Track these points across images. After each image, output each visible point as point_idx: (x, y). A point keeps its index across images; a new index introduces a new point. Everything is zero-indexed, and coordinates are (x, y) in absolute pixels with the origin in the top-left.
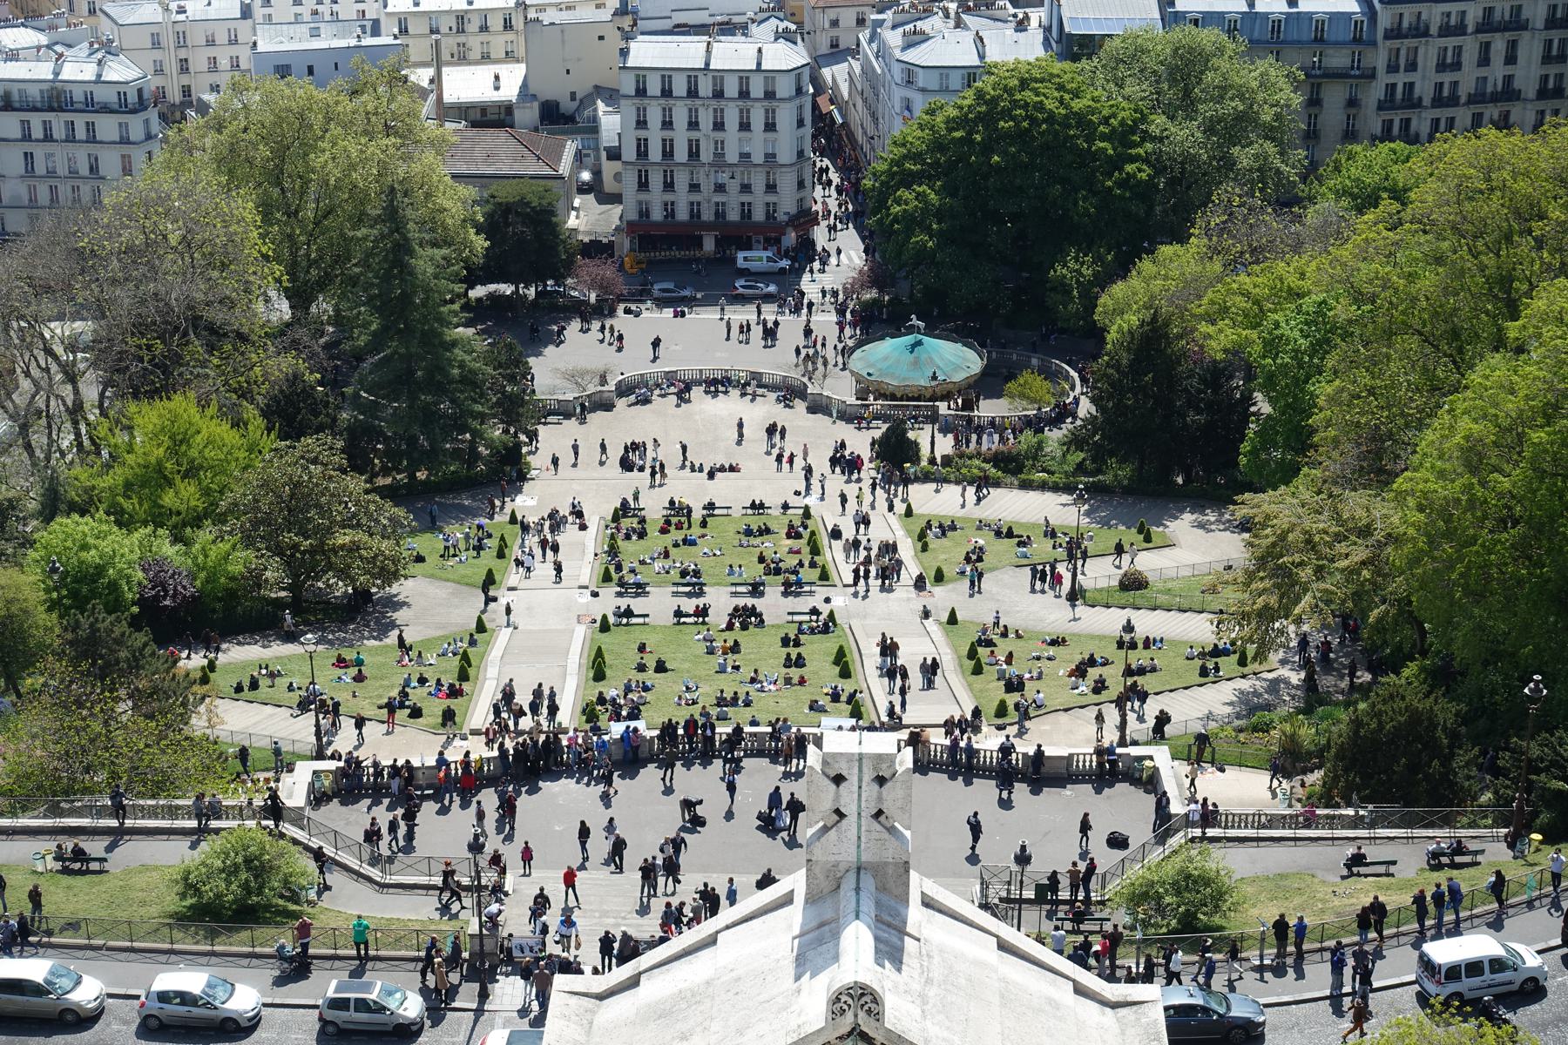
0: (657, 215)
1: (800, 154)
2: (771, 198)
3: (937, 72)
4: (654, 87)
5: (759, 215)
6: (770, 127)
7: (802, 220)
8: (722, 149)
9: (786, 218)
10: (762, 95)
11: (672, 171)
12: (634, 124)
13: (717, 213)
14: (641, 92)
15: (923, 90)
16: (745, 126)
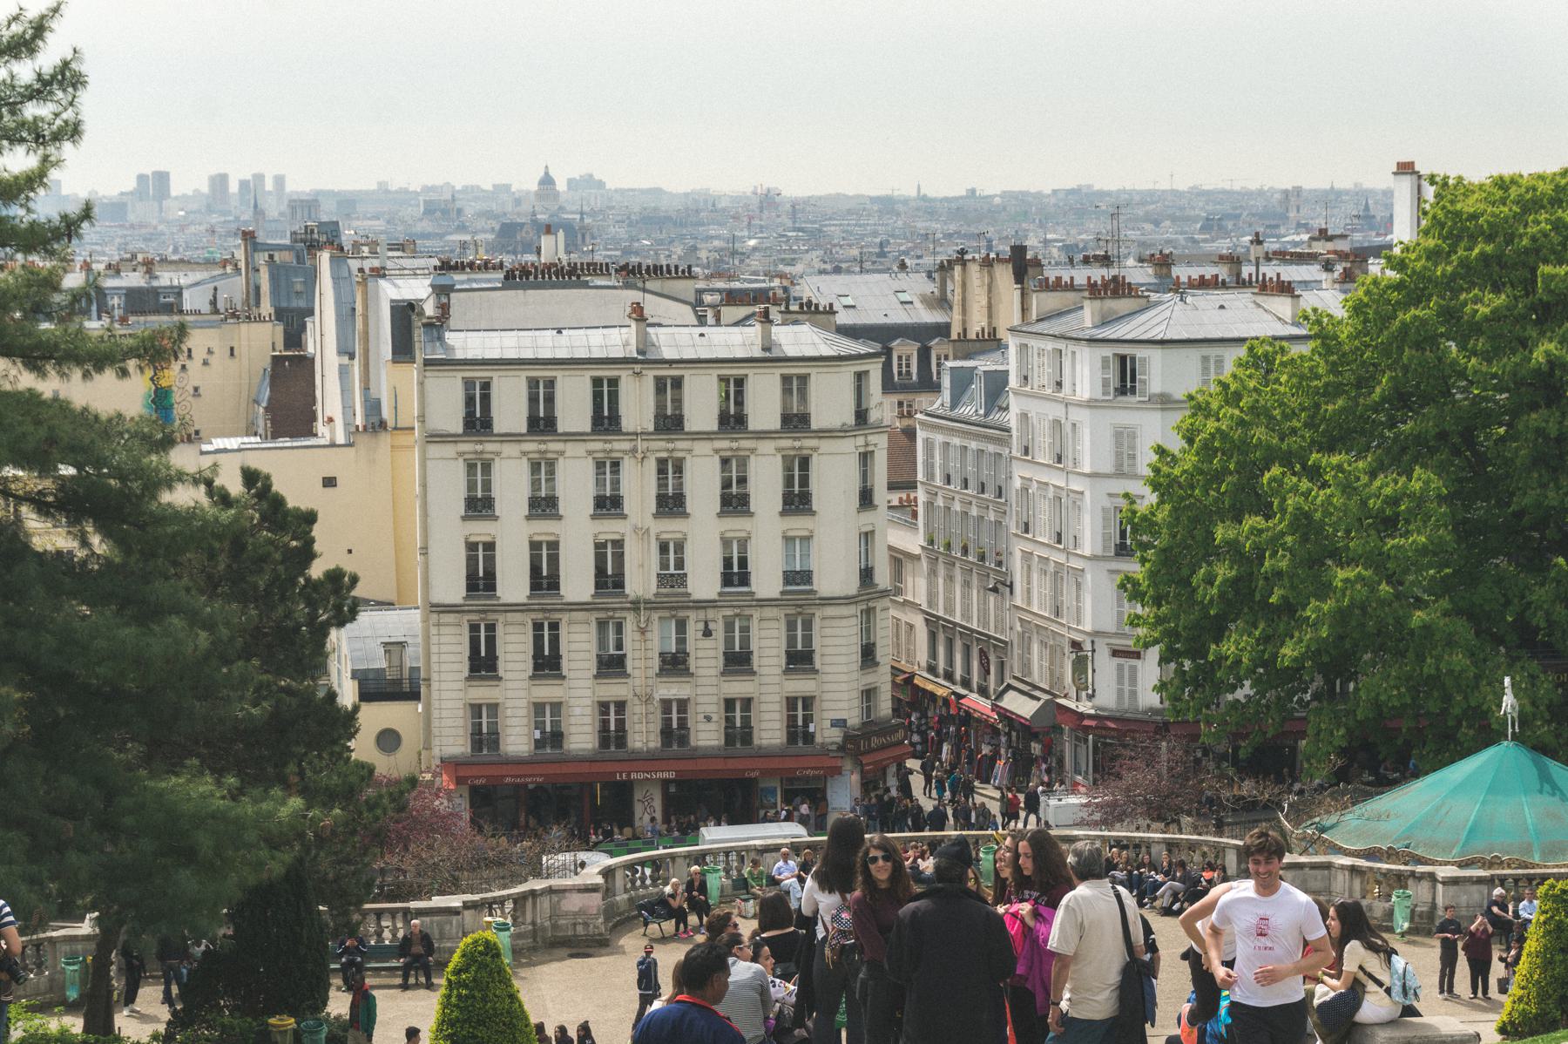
0: (517, 740)
1: (867, 574)
2: (801, 686)
3: (1194, 355)
4: (510, 409)
5: (770, 731)
6: (797, 500)
7: (875, 742)
8: (680, 564)
9: (835, 735)
10: (775, 423)
11: (554, 626)
12: (461, 509)
13: (666, 732)
14: (478, 422)
15: (1164, 402)
16: (734, 502)
